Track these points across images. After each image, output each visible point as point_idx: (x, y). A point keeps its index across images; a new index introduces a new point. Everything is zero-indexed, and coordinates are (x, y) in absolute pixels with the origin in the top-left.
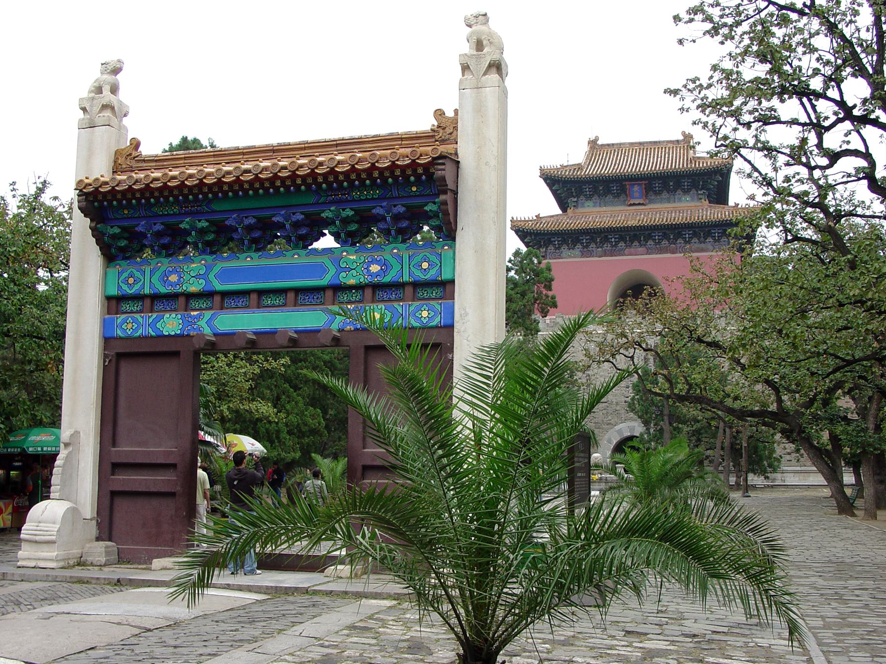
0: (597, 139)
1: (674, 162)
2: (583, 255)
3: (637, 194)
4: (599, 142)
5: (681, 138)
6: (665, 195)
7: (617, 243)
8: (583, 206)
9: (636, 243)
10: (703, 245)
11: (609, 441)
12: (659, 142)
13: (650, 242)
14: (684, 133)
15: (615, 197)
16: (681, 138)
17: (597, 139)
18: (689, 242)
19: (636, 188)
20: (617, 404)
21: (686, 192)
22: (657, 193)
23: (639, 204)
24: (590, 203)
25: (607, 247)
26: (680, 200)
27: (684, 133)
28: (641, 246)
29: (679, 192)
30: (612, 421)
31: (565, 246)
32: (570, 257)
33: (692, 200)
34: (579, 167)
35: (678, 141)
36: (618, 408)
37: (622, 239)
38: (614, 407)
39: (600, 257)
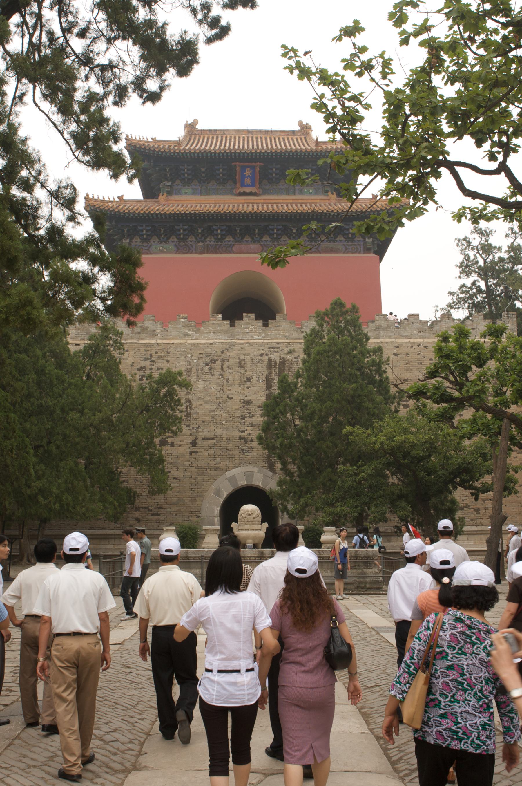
0: (196, 122)
2: (178, 250)
3: (248, 181)
4: (199, 127)
5: (297, 128)
7: (224, 236)
8: (179, 193)
9: (248, 238)
10: (332, 245)
11: (218, 493)
12: (272, 131)
13: (266, 238)
14: (300, 123)
16: (297, 128)
17: (196, 122)
20: (229, 440)
23: (251, 194)
24: (189, 190)
25: (211, 241)
27: (300, 123)
28: (254, 242)
30: (222, 465)
31: (155, 239)
32: (161, 252)
34: (178, 143)
35: (293, 132)
36: (230, 446)
37: (230, 231)
38: (224, 445)
39: (201, 253)
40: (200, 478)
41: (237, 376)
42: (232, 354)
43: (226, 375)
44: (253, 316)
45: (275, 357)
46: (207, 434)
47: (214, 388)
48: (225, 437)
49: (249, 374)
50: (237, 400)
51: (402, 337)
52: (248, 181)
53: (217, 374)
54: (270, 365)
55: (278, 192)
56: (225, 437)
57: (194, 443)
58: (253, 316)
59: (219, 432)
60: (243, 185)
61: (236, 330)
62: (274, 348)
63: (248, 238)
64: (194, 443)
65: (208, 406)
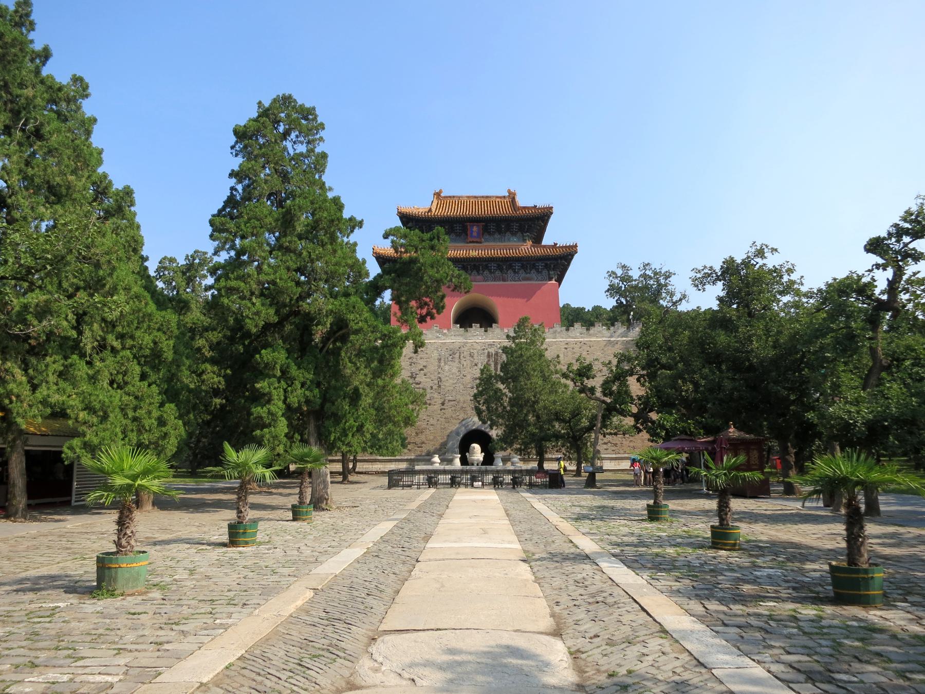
0: (441, 191)
1: (505, 211)
3: (475, 234)
6: (497, 236)
10: (528, 275)
14: (509, 191)
15: (457, 236)
17: (441, 191)
18: (518, 273)
19: (475, 229)
20: (464, 402)
21: (514, 234)
22: (489, 233)
26: (509, 240)
27: (509, 191)
28: (479, 274)
29: (508, 234)
33: (519, 241)
35: (504, 197)
36: (465, 405)
38: (461, 405)
40: (446, 425)
41: (469, 362)
42: (466, 349)
43: (463, 362)
44: (478, 325)
45: (492, 350)
46: (450, 398)
47: (455, 370)
48: (462, 399)
49: (476, 361)
50: (469, 377)
51: (570, 337)
52: (475, 234)
53: (457, 361)
54: (489, 355)
55: (494, 240)
56: (462, 399)
57: (443, 404)
58: (478, 325)
59: (458, 397)
60: (472, 236)
61: (469, 334)
62: (491, 345)
63: (475, 272)
64: (443, 404)
65: (451, 381)
